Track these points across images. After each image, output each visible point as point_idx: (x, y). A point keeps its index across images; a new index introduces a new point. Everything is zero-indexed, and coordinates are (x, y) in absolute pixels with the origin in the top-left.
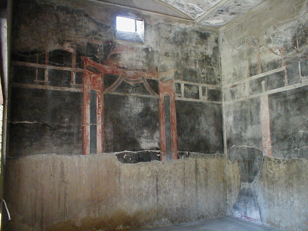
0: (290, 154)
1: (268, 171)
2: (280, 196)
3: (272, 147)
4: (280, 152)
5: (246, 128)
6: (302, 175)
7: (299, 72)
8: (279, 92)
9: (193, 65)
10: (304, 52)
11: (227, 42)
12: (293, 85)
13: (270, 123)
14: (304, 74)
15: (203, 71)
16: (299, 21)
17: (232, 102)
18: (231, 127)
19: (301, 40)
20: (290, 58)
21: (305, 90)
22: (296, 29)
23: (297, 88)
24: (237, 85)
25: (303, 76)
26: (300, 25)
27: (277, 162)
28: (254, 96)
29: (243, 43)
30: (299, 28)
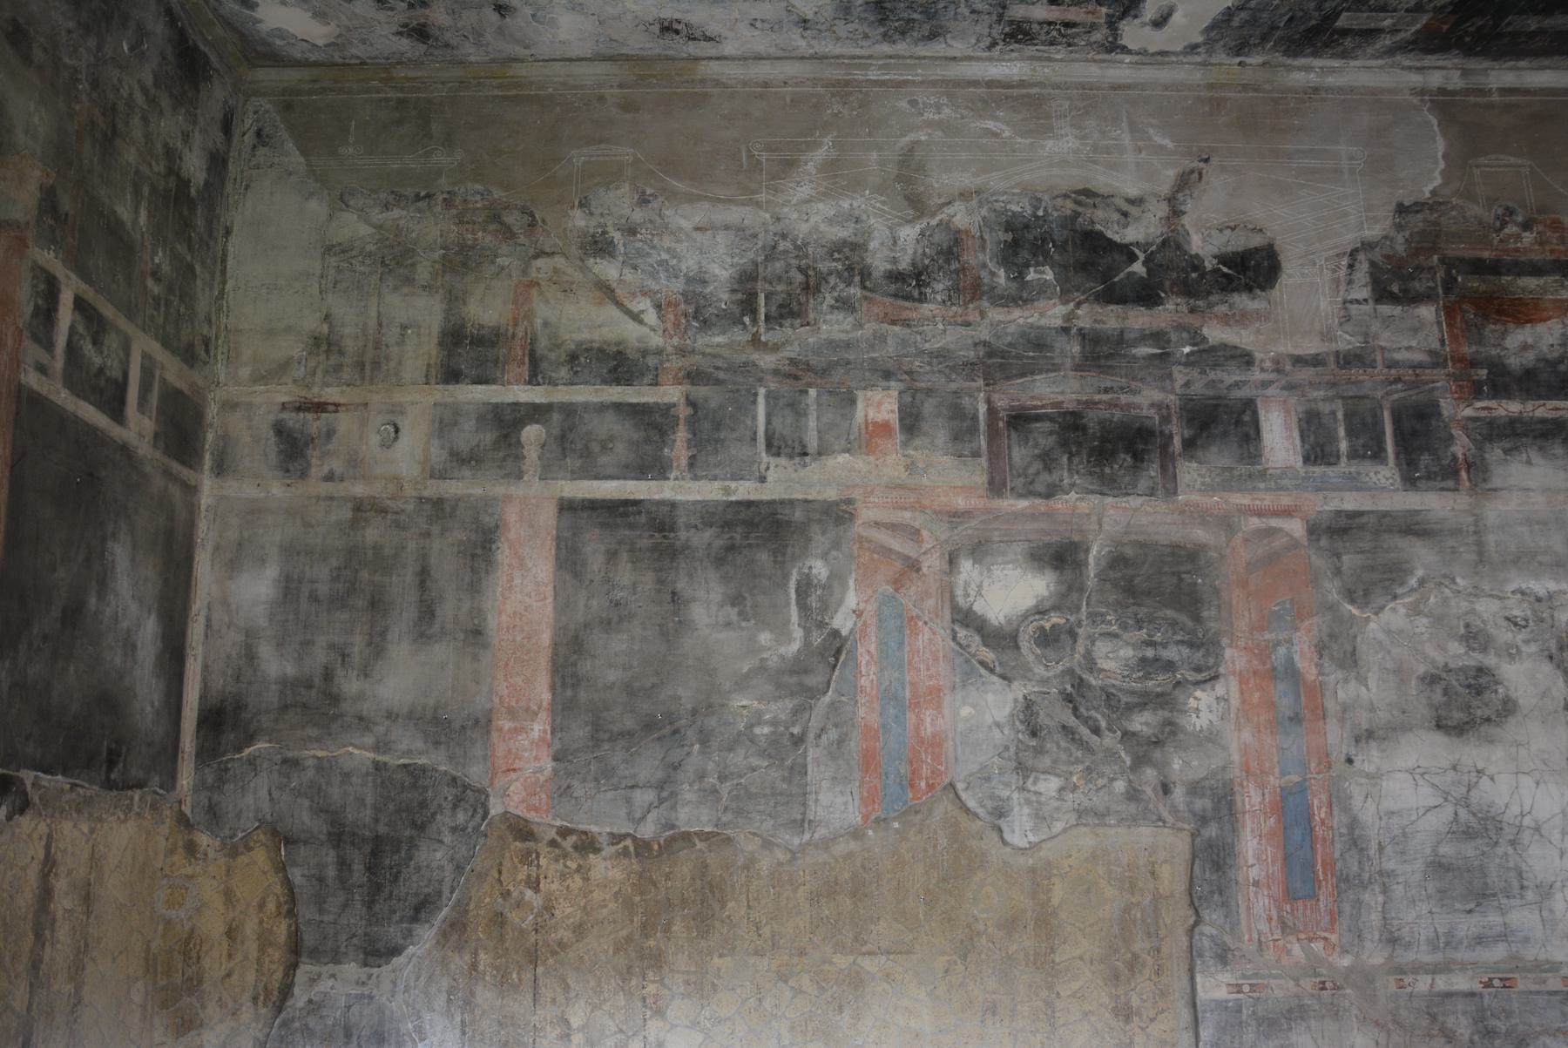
0: (673, 808)
1: (506, 895)
2: (576, 1022)
3: (555, 771)
4: (610, 795)
5: (377, 646)
6: (723, 907)
7: (755, 433)
8: (632, 497)
9: (129, 197)
10: (793, 355)
11: (296, 159)
12: (717, 484)
13: (555, 645)
14: (779, 448)
15: (157, 260)
17: (277, 490)
18: (250, 634)
19: (779, 299)
20: (714, 356)
21: (779, 517)
23: (738, 503)
24: (337, 405)
25: (778, 455)
27: (571, 850)
28: (452, 488)
29: (418, 198)
30: (774, 247)
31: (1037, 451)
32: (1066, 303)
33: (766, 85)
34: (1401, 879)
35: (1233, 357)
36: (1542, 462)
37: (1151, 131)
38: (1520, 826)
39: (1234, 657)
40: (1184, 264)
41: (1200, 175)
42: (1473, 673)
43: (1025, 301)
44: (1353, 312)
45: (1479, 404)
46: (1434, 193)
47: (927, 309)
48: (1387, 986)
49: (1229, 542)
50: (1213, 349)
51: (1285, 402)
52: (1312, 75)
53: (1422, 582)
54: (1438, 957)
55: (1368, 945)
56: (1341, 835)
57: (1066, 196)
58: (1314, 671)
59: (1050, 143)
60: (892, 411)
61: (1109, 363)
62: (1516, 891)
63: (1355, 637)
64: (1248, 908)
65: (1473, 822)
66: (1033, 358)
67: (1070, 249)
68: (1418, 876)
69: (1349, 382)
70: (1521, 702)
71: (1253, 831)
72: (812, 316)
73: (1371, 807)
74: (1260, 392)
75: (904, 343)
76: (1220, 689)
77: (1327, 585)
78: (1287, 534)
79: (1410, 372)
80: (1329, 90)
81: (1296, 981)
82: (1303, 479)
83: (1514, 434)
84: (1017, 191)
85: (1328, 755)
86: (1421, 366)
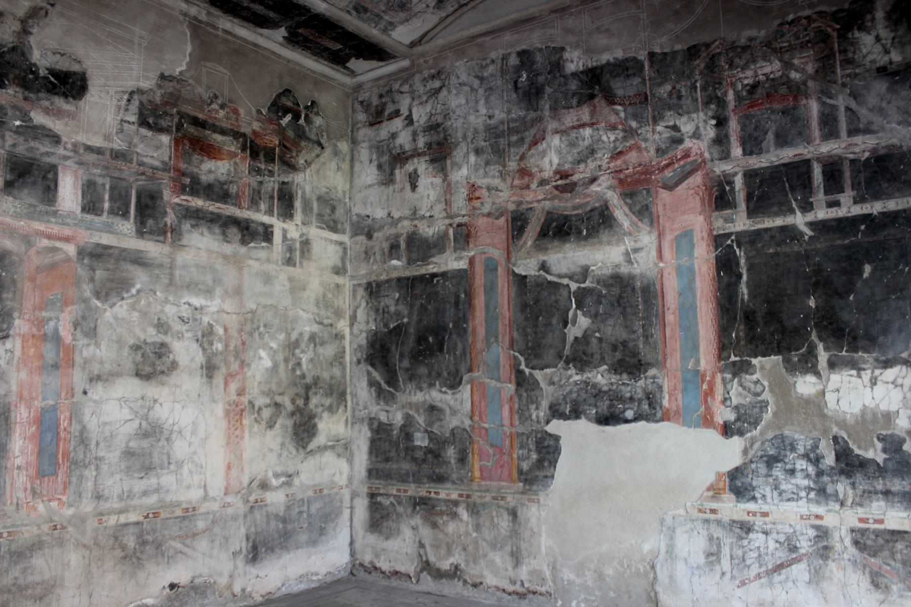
34: (107, 462)
35: (47, 136)
36: (208, 235)
38: (172, 431)
39: (20, 325)
42: (158, 346)
44: (125, 128)
45: (183, 197)
46: (181, 73)
48: (92, 524)
49: (27, 251)
50: (35, 127)
51: (76, 171)
53: (139, 292)
54: (123, 504)
55: (85, 501)
56: (75, 437)
58: (70, 337)
62: (166, 465)
63: (97, 320)
64: (12, 484)
65: (149, 428)
68: (116, 460)
69: (116, 168)
70: (180, 363)
71: (20, 435)
73: (95, 420)
74: (61, 162)
76: (9, 344)
77: (85, 287)
78: (65, 253)
81: (39, 526)
82: (80, 221)
83: (197, 217)
85: (72, 389)
86: (156, 168)
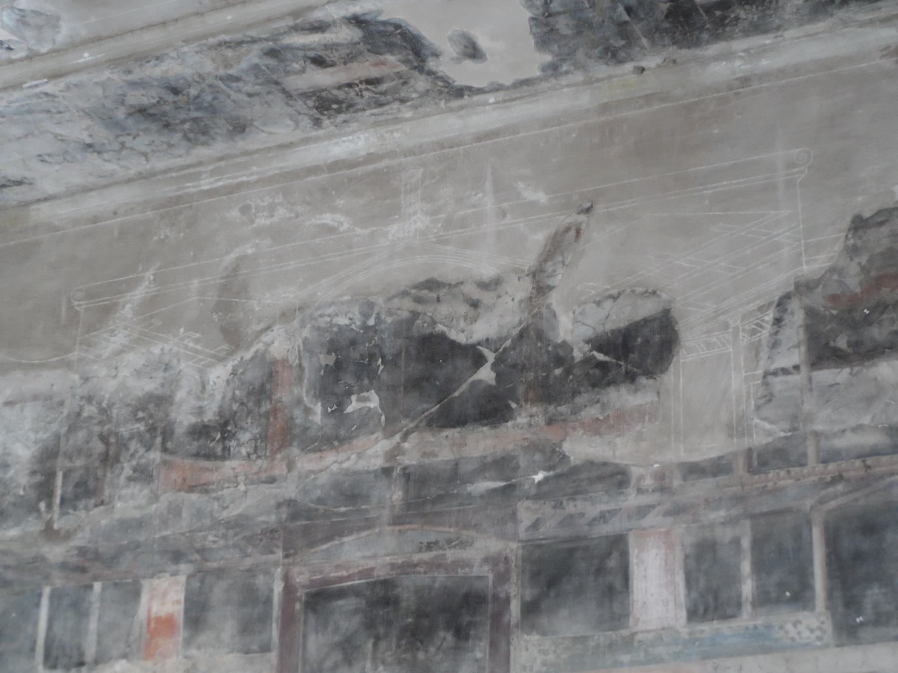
14: (57, 658)
16: (86, 380)
19: (76, 477)
22: (66, 411)
25: (54, 667)
26: (89, 399)
30: (79, 414)
31: (337, 638)
32: (389, 435)
33: (95, 219)
35: (600, 478)
37: (521, 185)
40: (545, 358)
41: (578, 232)
43: (342, 441)
47: (230, 467)
50: (575, 470)
51: (667, 533)
52: (738, 63)
57: (404, 294)
59: (394, 230)
60: (178, 602)
61: (437, 508)
66: (344, 514)
67: (402, 363)
72: (107, 492)
75: (199, 514)
79: (858, 463)
80: (766, 76)
84: (346, 298)
86: (875, 452)
